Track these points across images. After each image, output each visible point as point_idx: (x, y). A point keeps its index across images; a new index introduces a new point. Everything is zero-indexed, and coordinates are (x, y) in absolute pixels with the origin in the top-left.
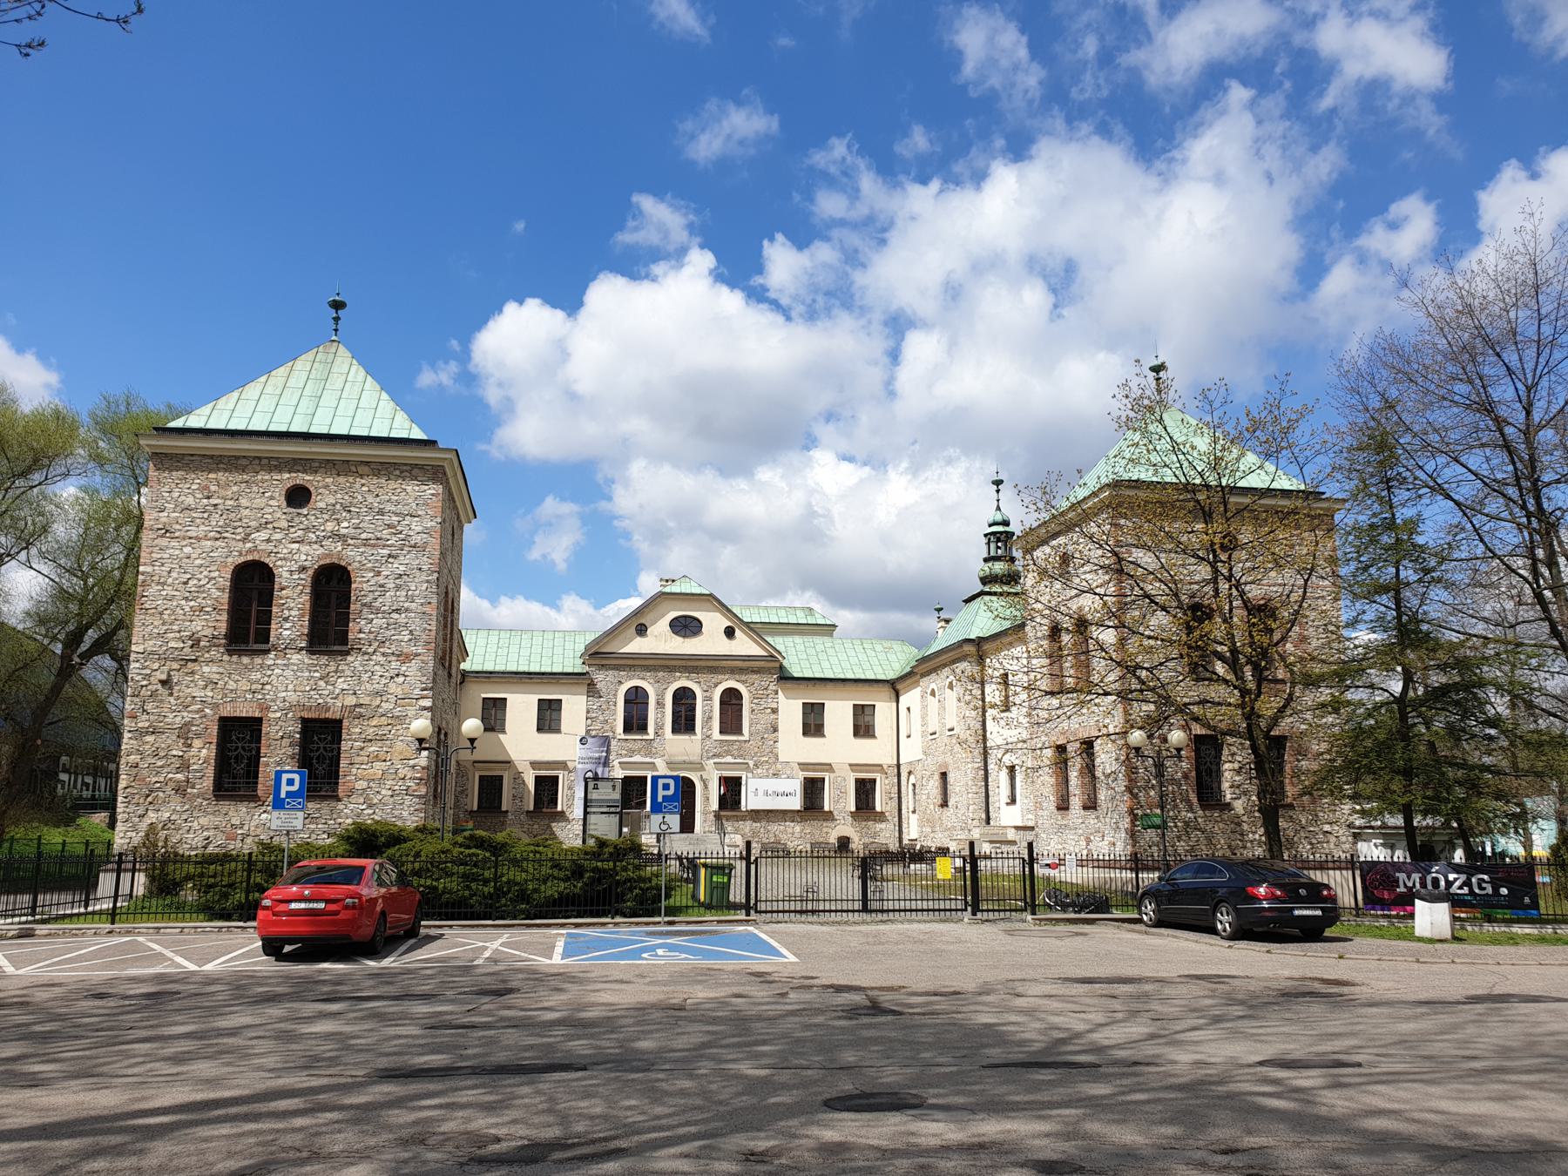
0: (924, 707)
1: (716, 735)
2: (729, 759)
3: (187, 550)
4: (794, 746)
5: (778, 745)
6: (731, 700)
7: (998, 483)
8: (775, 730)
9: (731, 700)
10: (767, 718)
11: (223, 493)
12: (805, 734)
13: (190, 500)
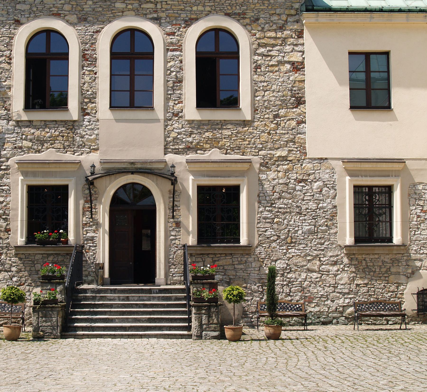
1: (190, 110)
5: (307, 127)
8: (300, 101)
10: (282, 79)
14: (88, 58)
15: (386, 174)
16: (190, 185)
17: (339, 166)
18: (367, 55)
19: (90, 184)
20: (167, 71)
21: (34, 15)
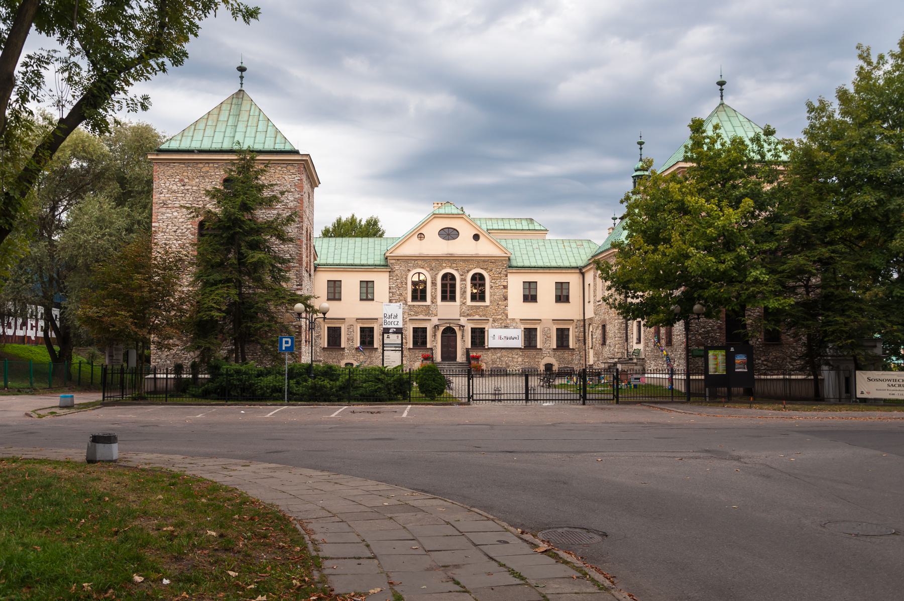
0: (595, 285)
1: (469, 302)
2: (477, 317)
3: (175, 214)
4: (517, 309)
5: (509, 308)
6: (478, 280)
7: (641, 144)
8: (506, 299)
9: (478, 280)
11: (191, 183)
12: (524, 301)
13: (175, 187)
14: (434, 284)
15: (535, 324)
16: (469, 327)
17: (518, 321)
18: (530, 283)
19: (436, 327)
20: (461, 288)
21: (414, 267)
